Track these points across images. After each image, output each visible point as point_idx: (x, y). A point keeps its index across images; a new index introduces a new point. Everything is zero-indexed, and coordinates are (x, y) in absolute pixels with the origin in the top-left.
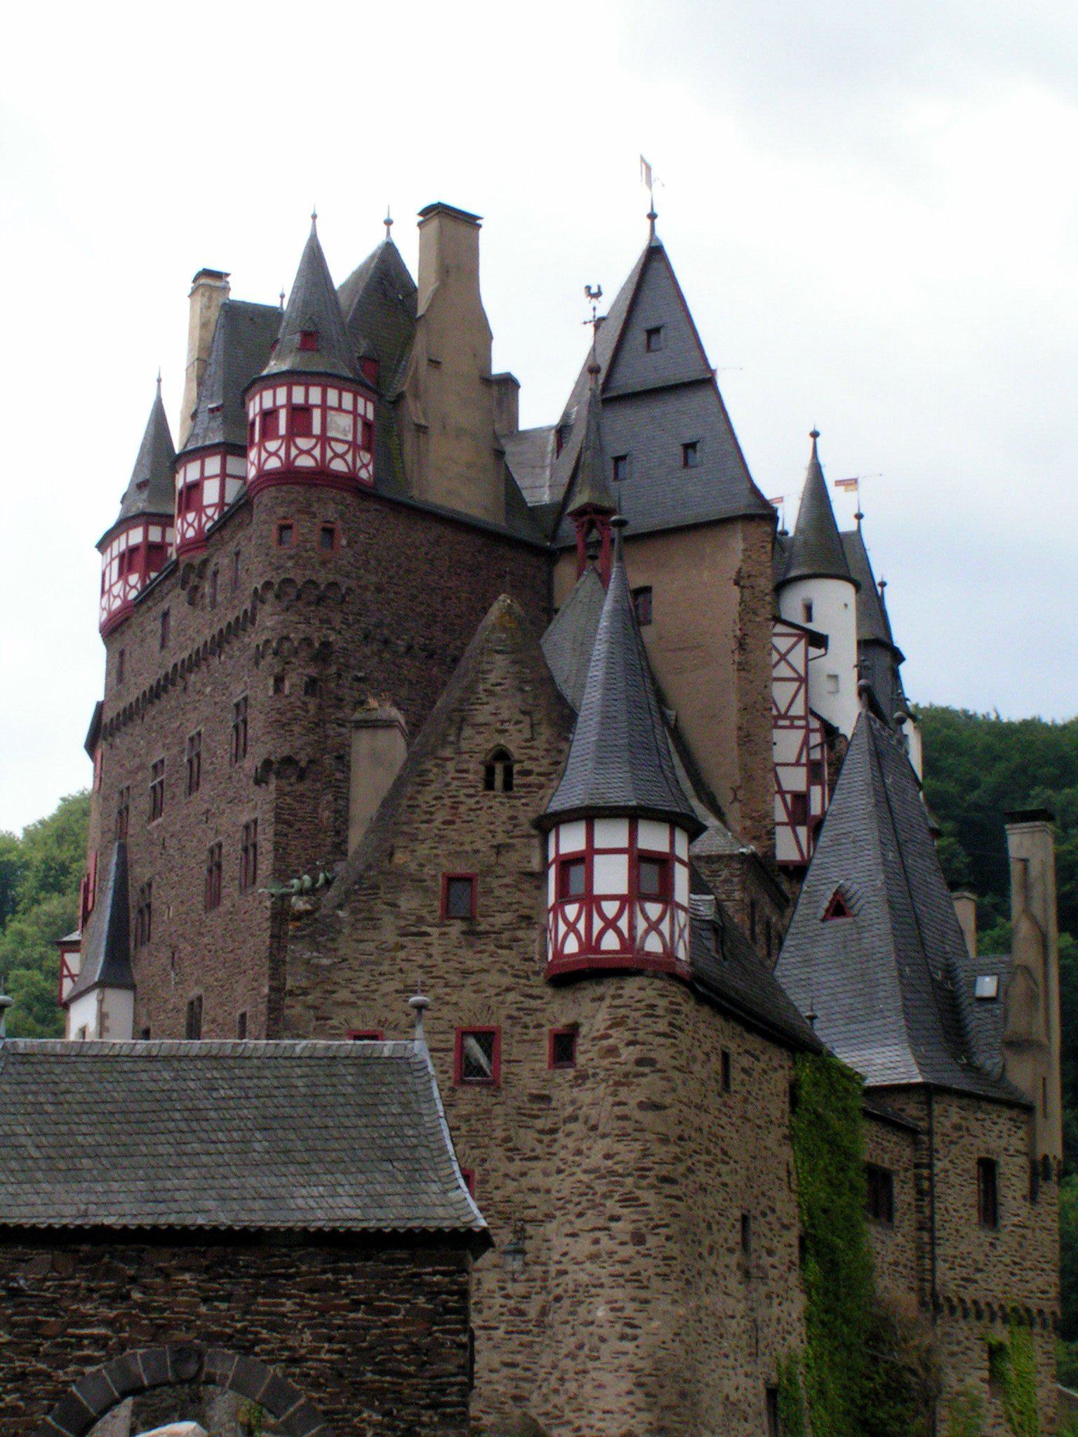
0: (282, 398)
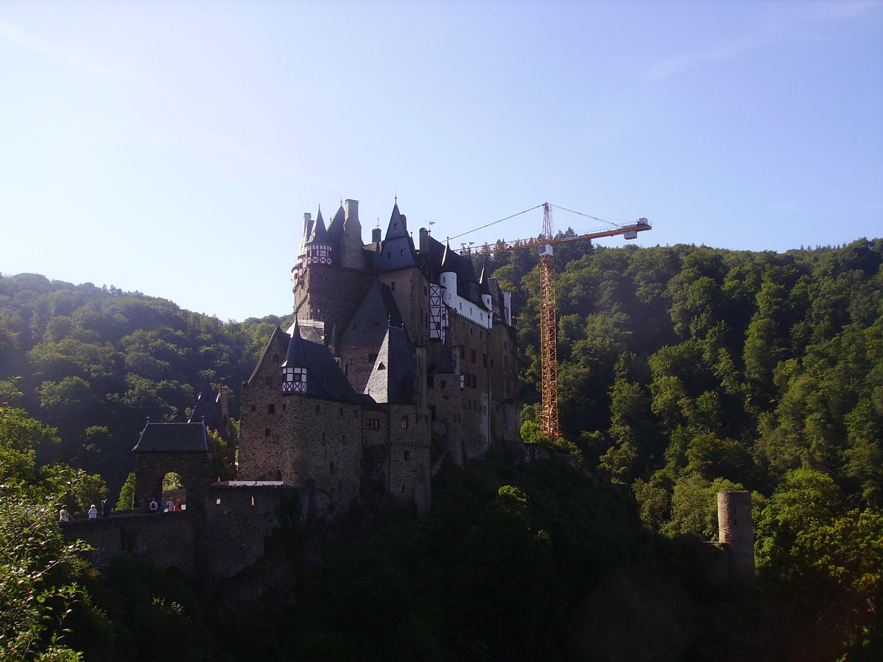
0: (310, 249)
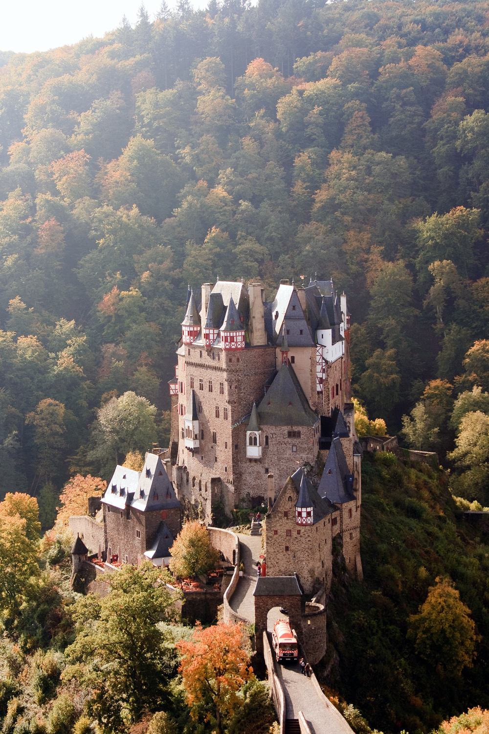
0: (228, 335)
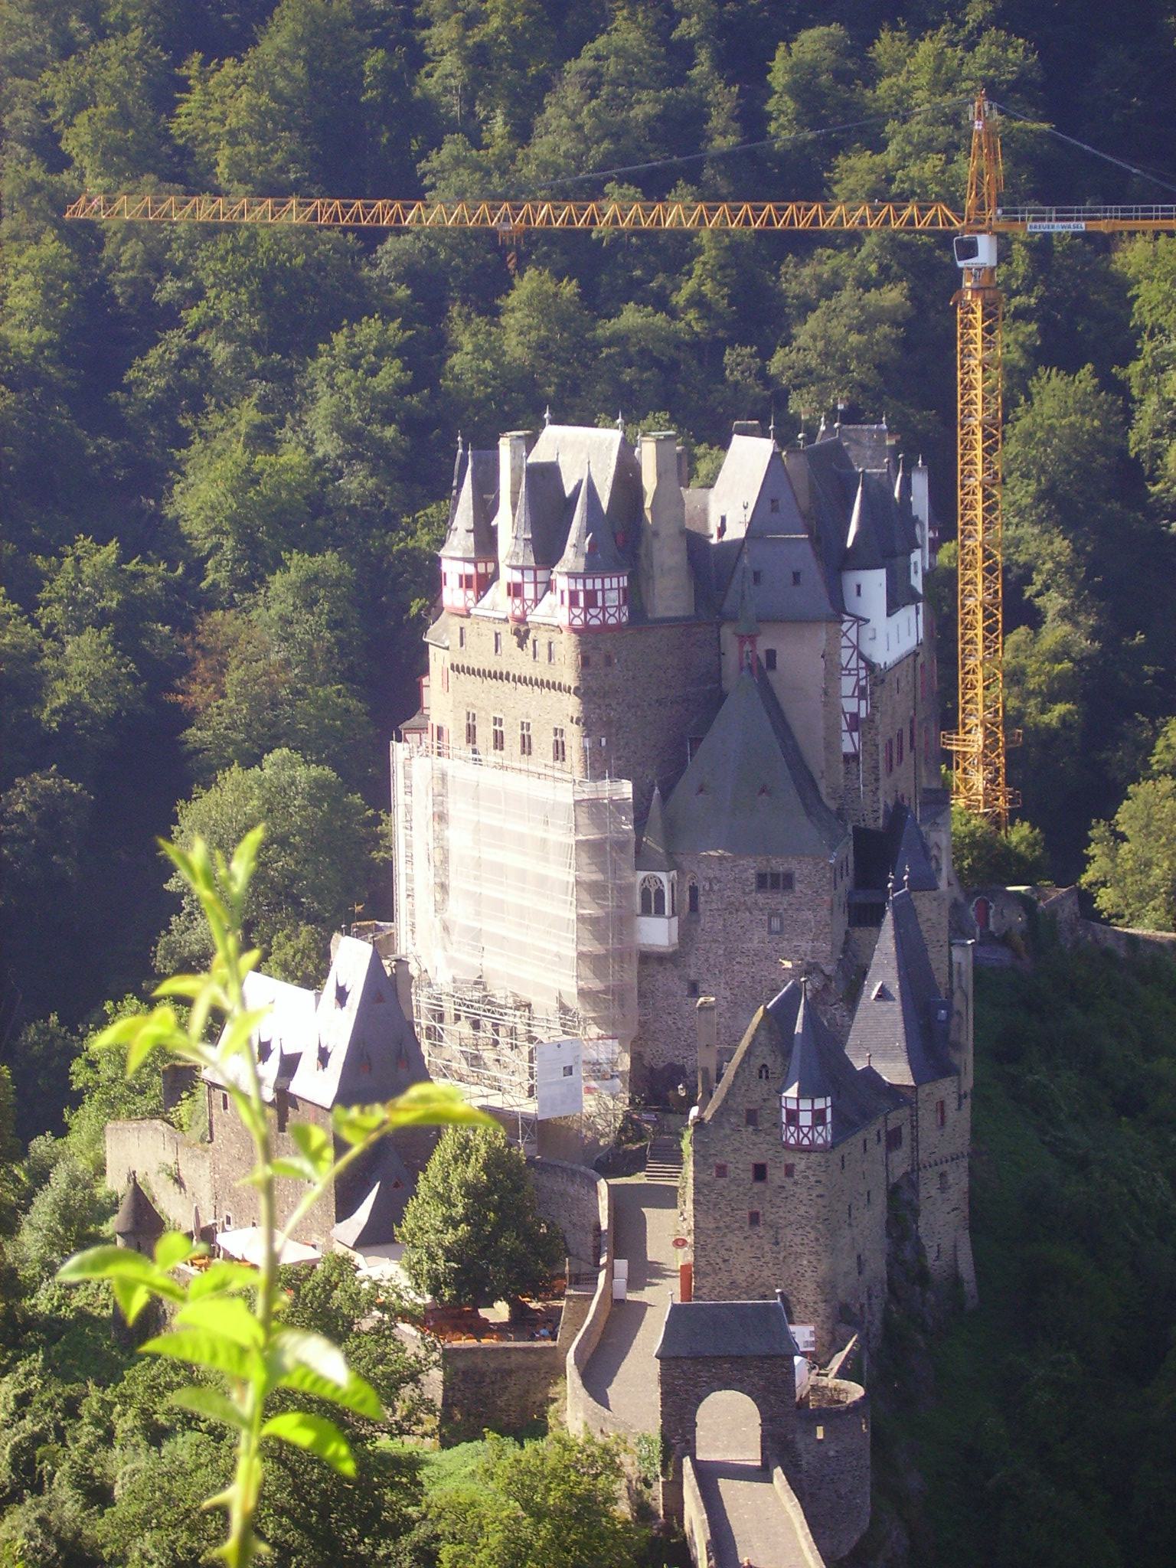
0: (580, 587)
